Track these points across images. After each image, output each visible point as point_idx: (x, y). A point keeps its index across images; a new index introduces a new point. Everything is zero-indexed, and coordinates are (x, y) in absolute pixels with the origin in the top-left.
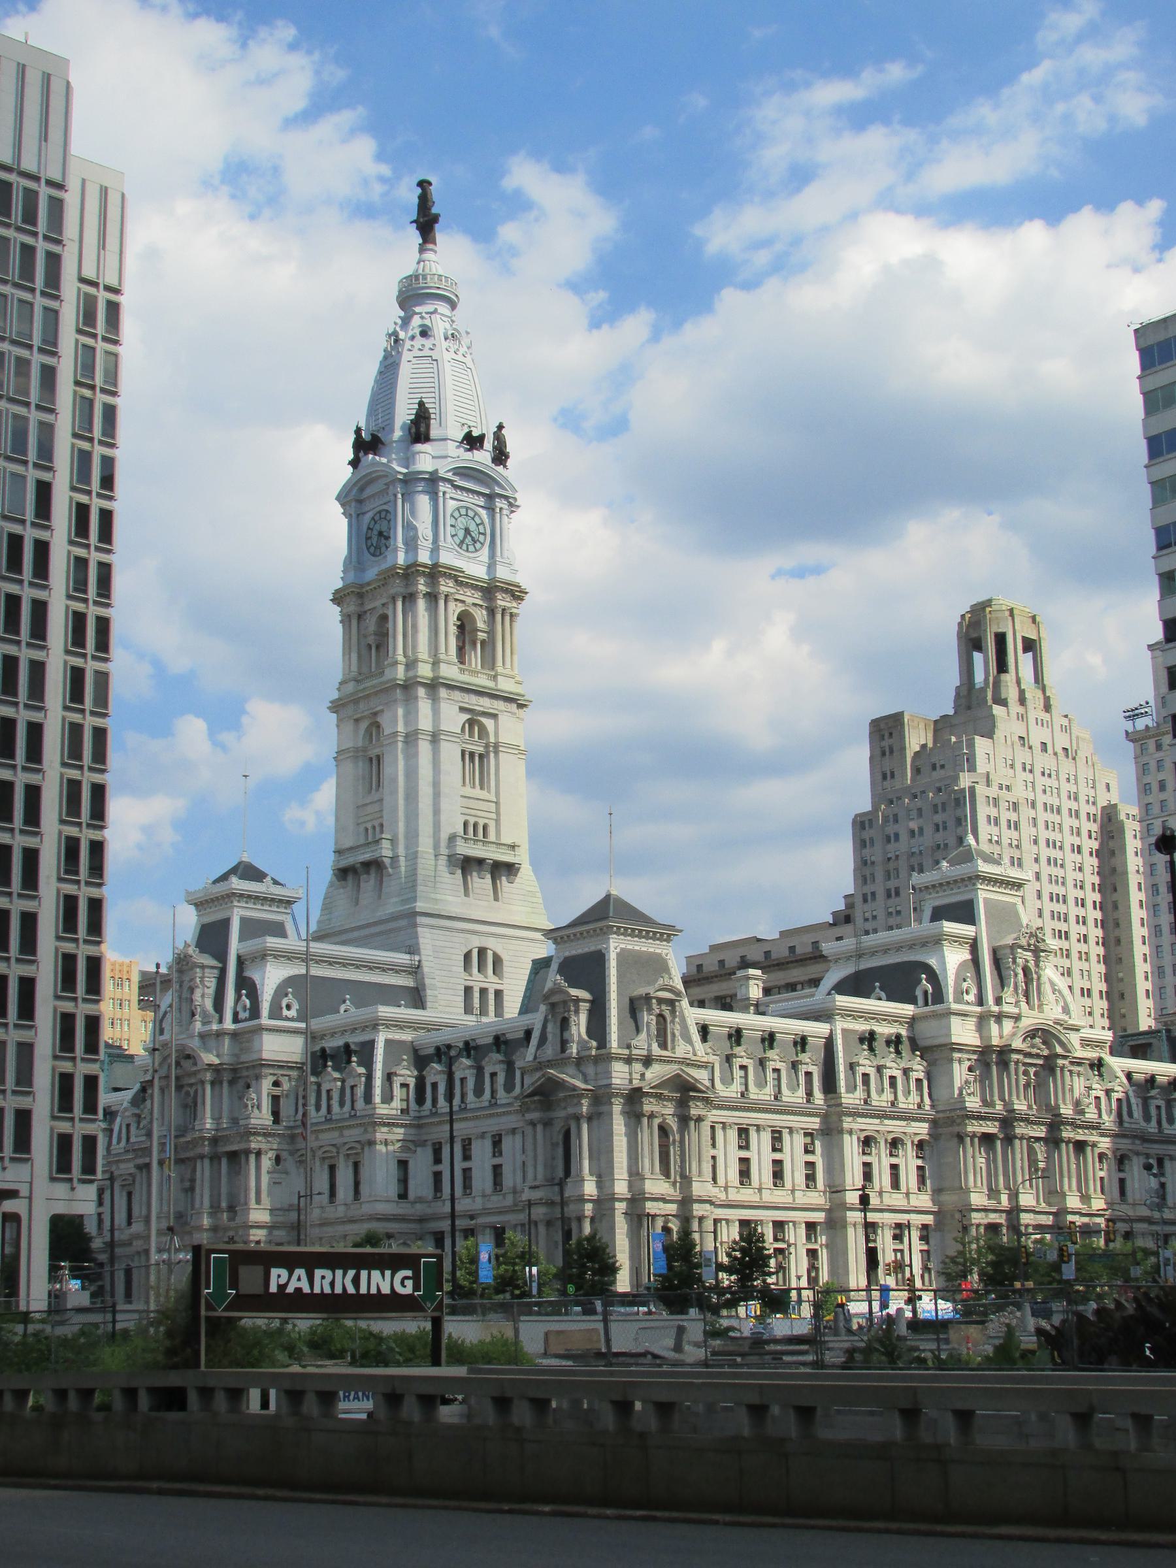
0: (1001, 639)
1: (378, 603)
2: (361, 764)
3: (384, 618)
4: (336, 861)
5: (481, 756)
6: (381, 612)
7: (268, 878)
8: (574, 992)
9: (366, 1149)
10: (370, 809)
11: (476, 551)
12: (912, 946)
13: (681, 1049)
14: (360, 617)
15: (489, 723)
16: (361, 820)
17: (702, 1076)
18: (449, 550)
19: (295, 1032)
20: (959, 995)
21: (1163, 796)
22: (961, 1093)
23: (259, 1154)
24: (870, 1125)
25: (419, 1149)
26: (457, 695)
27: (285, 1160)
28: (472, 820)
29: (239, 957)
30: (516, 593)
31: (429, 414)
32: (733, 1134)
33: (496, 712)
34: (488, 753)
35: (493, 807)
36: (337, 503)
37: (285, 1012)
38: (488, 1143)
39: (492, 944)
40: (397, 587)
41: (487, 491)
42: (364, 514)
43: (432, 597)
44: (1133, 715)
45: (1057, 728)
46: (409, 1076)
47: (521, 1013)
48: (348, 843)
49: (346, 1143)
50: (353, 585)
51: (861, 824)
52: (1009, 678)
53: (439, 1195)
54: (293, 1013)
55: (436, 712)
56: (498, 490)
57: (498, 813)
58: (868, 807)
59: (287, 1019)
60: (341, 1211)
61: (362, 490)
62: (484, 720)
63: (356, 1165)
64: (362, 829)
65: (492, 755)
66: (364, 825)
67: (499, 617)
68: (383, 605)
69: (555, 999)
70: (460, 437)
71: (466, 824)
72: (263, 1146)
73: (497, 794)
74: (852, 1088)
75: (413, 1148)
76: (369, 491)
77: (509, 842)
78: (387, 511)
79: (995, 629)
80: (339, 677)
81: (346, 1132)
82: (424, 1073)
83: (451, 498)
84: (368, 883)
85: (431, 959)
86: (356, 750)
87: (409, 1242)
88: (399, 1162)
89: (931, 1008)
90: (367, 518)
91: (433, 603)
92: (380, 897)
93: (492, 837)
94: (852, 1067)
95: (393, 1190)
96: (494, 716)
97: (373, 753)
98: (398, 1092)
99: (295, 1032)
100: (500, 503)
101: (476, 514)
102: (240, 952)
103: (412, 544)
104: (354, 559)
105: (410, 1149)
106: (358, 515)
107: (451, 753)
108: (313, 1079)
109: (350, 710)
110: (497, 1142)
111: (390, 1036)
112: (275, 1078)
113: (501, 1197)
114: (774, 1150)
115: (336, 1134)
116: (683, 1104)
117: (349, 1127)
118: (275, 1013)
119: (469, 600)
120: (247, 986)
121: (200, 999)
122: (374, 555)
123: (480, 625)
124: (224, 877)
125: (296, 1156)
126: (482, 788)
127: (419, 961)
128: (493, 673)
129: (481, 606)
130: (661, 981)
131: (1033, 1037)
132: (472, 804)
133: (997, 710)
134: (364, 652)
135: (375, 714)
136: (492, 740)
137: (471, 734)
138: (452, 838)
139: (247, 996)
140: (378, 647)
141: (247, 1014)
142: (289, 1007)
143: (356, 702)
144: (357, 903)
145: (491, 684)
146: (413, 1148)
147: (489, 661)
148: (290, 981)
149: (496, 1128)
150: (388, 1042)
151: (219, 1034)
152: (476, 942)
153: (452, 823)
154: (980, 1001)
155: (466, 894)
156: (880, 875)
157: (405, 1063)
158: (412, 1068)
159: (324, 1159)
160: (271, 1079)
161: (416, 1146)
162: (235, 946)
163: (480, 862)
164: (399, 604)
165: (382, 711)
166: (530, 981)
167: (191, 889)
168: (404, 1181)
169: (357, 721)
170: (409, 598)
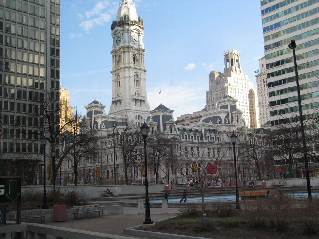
0: (232, 60)
1: (119, 53)
3: (120, 56)
5: (138, 81)
8: (154, 122)
10: (118, 91)
12: (217, 113)
13: (174, 133)
14: (115, 56)
15: (139, 74)
17: (178, 137)
18: (131, 43)
20: (225, 122)
21: (261, 87)
22: (226, 140)
24: (209, 146)
26: (134, 70)
28: (136, 92)
29: (94, 118)
30: (143, 50)
32: (184, 148)
39: (141, 115)
40: (122, 50)
43: (128, 52)
44: (256, 72)
45: (242, 75)
48: (114, 97)
50: (114, 50)
51: (207, 93)
52: (233, 67)
54: (104, 128)
55: (130, 73)
57: (141, 91)
58: (209, 90)
59: (103, 128)
61: (115, 33)
62: (138, 74)
69: (151, 124)
71: (135, 93)
73: (141, 87)
74: (206, 139)
76: (116, 33)
77: (143, 96)
78: (120, 36)
79: (231, 58)
80: (112, 67)
84: (118, 104)
86: (115, 80)
89: (220, 125)
90: (117, 37)
93: (140, 95)
94: (205, 136)
96: (140, 73)
97: (118, 81)
99: (105, 131)
103: (124, 42)
107: (132, 80)
108: (108, 139)
109: (114, 73)
119: (135, 52)
120: (96, 123)
122: (118, 44)
123: (137, 57)
124: (91, 103)
126: (138, 86)
130: (170, 120)
131: (239, 129)
132: (137, 89)
133: (231, 72)
134: (116, 62)
136: (140, 78)
137: (136, 77)
138: (133, 96)
140: (119, 61)
142: (103, 126)
143: (115, 71)
145: (139, 67)
147: (139, 64)
148: (104, 122)
152: (138, 114)
153: (133, 93)
154: (229, 123)
155: (136, 106)
156: (211, 102)
159: (110, 153)
163: (138, 100)
164: (122, 53)
165: (120, 73)
167: (86, 105)
169: (115, 75)
170: (124, 52)
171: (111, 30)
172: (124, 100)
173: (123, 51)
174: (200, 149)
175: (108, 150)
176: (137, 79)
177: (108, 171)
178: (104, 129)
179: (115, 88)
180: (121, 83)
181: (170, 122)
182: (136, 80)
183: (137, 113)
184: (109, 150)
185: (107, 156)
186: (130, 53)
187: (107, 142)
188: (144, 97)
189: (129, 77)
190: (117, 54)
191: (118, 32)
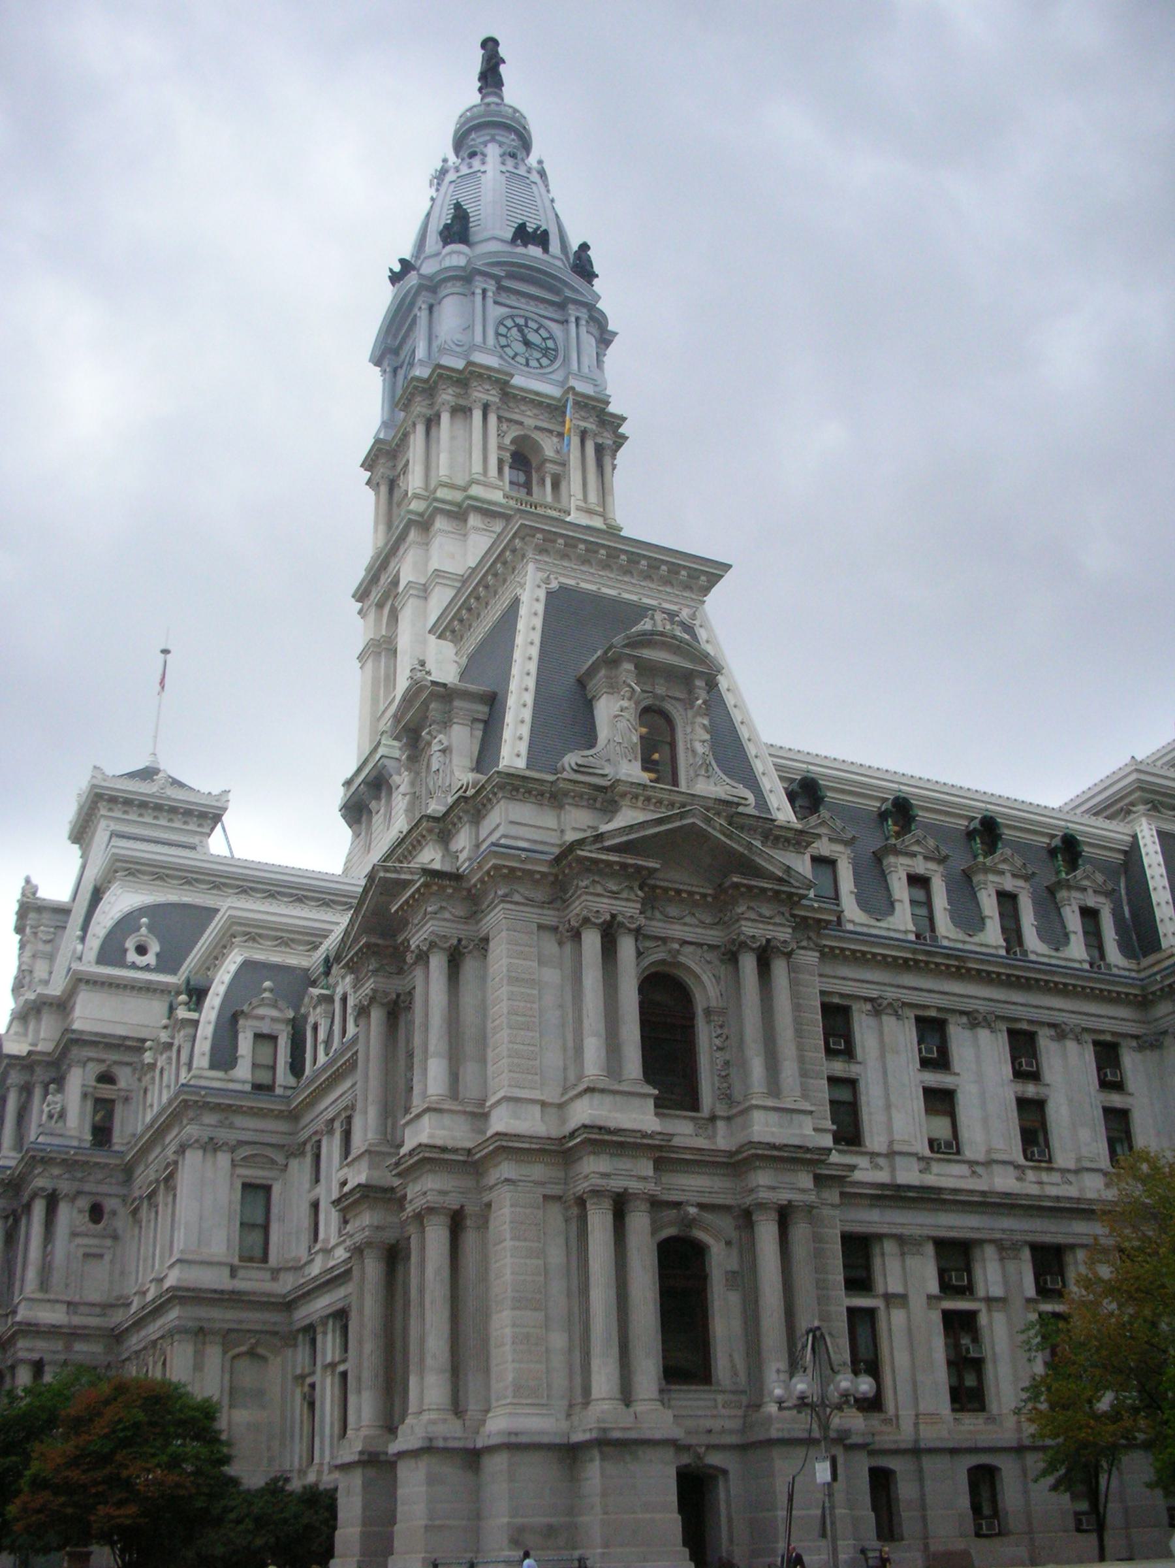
7: (161, 775)
19: (148, 989)
25: (294, 1164)
27: (114, 1213)
31: (468, 213)
36: (371, 365)
37: (132, 956)
41: (556, 299)
46: (273, 1020)
54: (150, 959)
56: (568, 293)
59: (134, 966)
70: (509, 234)
72: (65, 1187)
83: (496, 303)
87: (260, 1350)
99: (148, 989)
100: (573, 311)
101: (541, 326)
105: (273, 1162)
111: (259, 956)
112: (102, 1068)
114: (1019, 1074)
118: (111, 952)
119: (530, 422)
123: (549, 452)
129: (551, 432)
142: (142, 950)
146: (280, 1158)
150: (247, 965)
157: (266, 995)
160: (94, 1070)
170: (431, 422)
173: (429, 412)
174: (1131, 1061)
178: (147, 968)
181: (648, 653)
186: (477, 415)
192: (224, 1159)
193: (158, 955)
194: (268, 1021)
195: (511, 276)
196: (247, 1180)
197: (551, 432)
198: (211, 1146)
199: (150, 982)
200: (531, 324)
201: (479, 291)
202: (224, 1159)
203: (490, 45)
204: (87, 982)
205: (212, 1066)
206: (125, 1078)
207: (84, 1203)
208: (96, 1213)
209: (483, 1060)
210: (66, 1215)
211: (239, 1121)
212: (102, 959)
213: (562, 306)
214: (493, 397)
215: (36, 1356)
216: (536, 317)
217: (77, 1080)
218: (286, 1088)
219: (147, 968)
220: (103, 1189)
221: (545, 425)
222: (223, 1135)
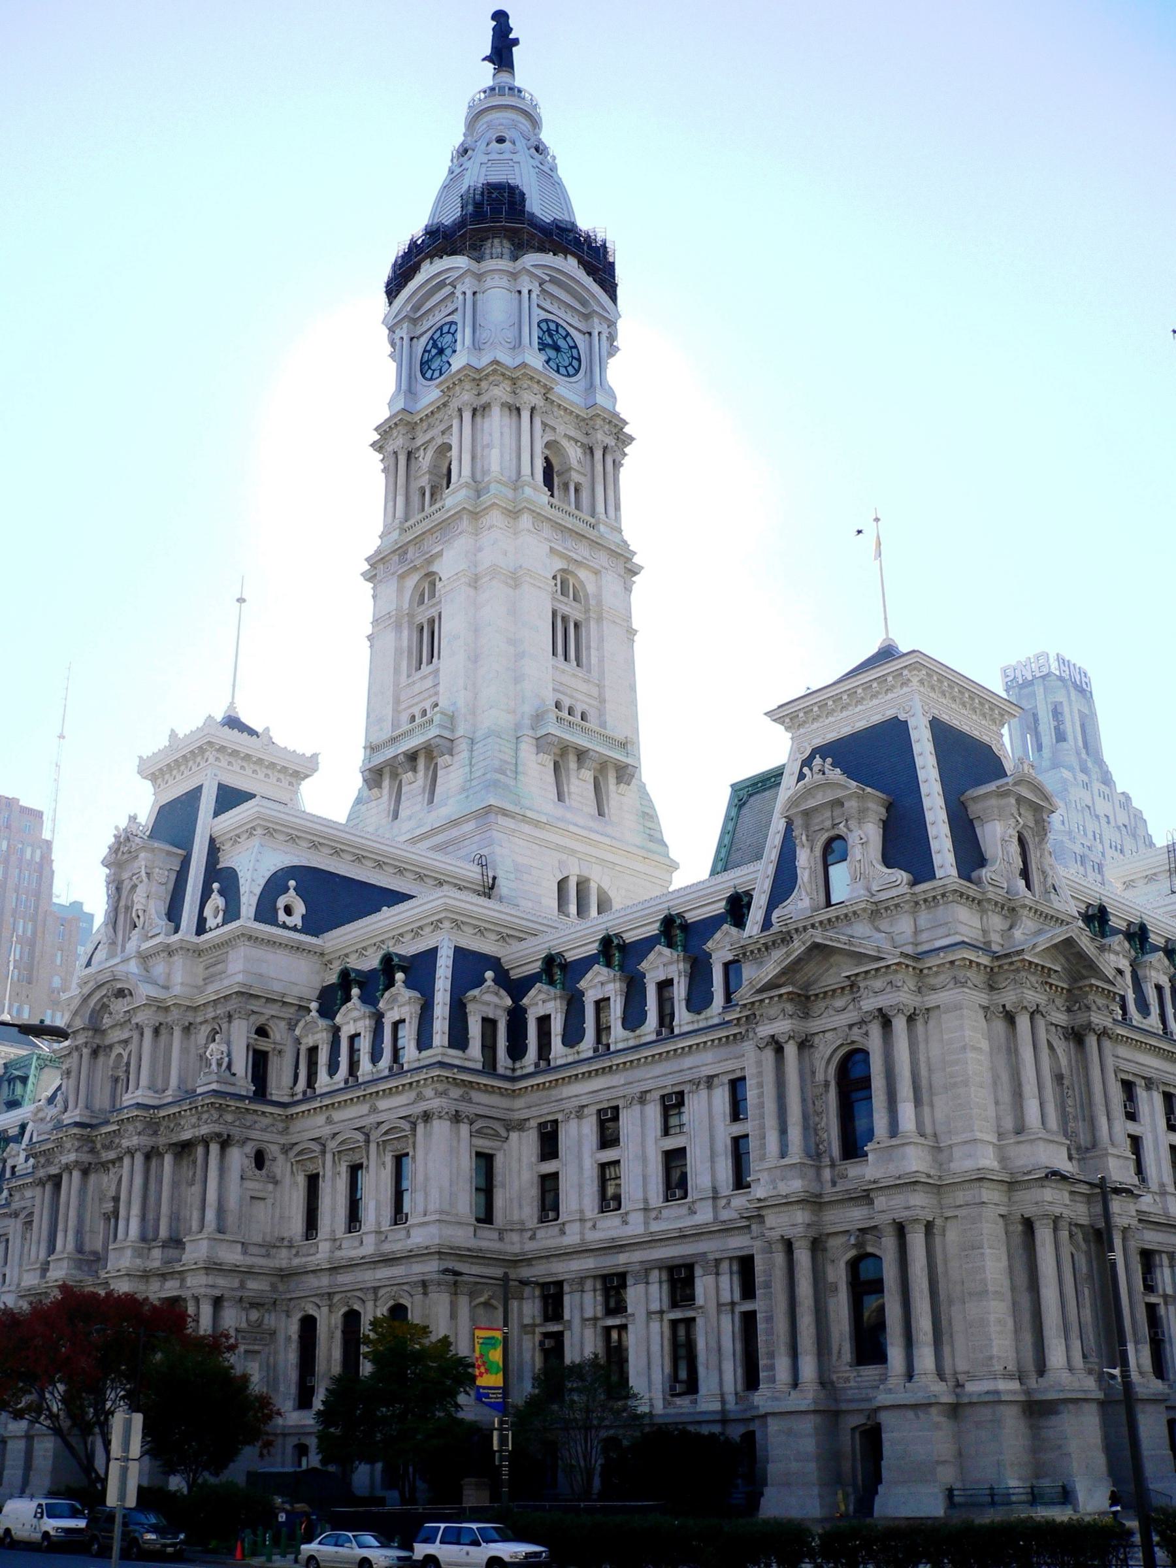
2: (405, 633)
4: (368, 759)
5: (576, 625)
6: (439, 441)
9: (420, 1128)
11: (569, 375)
16: (403, 706)
23: (225, 1143)
25: (514, 1136)
27: (274, 1159)
28: (566, 702)
29: (212, 840)
33: (599, 568)
34: (588, 619)
35: (595, 692)
38: (653, 1112)
42: (418, 338)
46: (496, 1006)
47: (714, 872)
49: (379, 1124)
53: (551, 1215)
54: (296, 920)
57: (602, 701)
59: (284, 926)
60: (369, 1247)
62: (583, 574)
63: (399, 1160)
64: (405, 717)
65: (593, 624)
66: (410, 711)
67: (598, 454)
68: (443, 433)
71: (558, 705)
72: (235, 1132)
75: (503, 1133)
81: (382, 1104)
82: (525, 1001)
85: (512, 876)
88: (479, 1155)
90: (424, 340)
91: (514, 418)
92: (431, 801)
93: (592, 724)
95: (465, 1203)
97: (422, 617)
98: (475, 1029)
99: (298, 948)
101: (568, 334)
102: (214, 830)
104: (404, 386)
105: (498, 1135)
106: (412, 339)
110: (673, 1104)
113: (684, 1211)
115: (364, 1109)
116: (1074, 999)
117: (389, 1092)
118: (266, 912)
121: (143, 901)
125: (292, 1154)
127: (494, 878)
128: (592, 520)
129: (577, 441)
134: (415, 498)
135: (430, 561)
138: (538, 718)
139: (221, 893)
141: (220, 919)
142: (288, 910)
144: (396, 816)
146: (503, 1133)
148: (293, 871)
149: (669, 1081)
151: (169, 951)
158: (503, 993)
161: (508, 1130)
162: (206, 824)
164: (467, 415)
165: (440, 554)
166: (728, 818)
167: (147, 753)
168: (486, 1188)
169: (402, 577)
171: (383, 298)
172: (462, 746)
175: (320, 1119)
176: (573, 611)
177: (308, 1325)
178: (294, 929)
179: (397, 670)
180: (452, 627)
182: (565, 619)
183: (572, 852)
184: (329, 1121)
185: (301, 1180)
186: (525, 415)
187: (313, 1051)
188: (623, 745)
189: (515, 579)
190: (419, 442)
191: (447, 290)
192: (464, 1129)
193: (303, 916)
194: (492, 1006)
195: (553, 281)
196: (479, 1150)
197: (577, 441)
198: (456, 1118)
199: (301, 942)
200: (560, 330)
201: (525, 292)
202: (464, 1129)
203: (500, 17)
204: (250, 938)
205: (451, 1046)
206: (278, 1032)
207: (250, 1149)
208: (260, 1159)
209: (932, 1106)
210: (238, 1158)
211: (476, 1096)
212: (258, 917)
213: (587, 317)
214: (538, 401)
215: (218, 1293)
216: (565, 325)
217: (240, 1034)
218: (506, 1068)
219: (294, 929)
220: (266, 1137)
221: (572, 433)
222: (466, 1108)
